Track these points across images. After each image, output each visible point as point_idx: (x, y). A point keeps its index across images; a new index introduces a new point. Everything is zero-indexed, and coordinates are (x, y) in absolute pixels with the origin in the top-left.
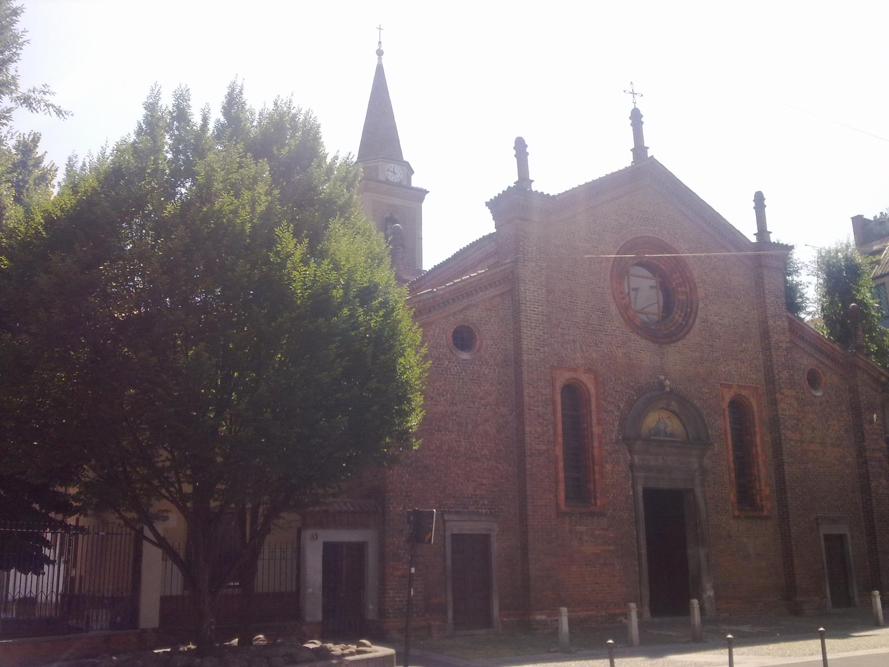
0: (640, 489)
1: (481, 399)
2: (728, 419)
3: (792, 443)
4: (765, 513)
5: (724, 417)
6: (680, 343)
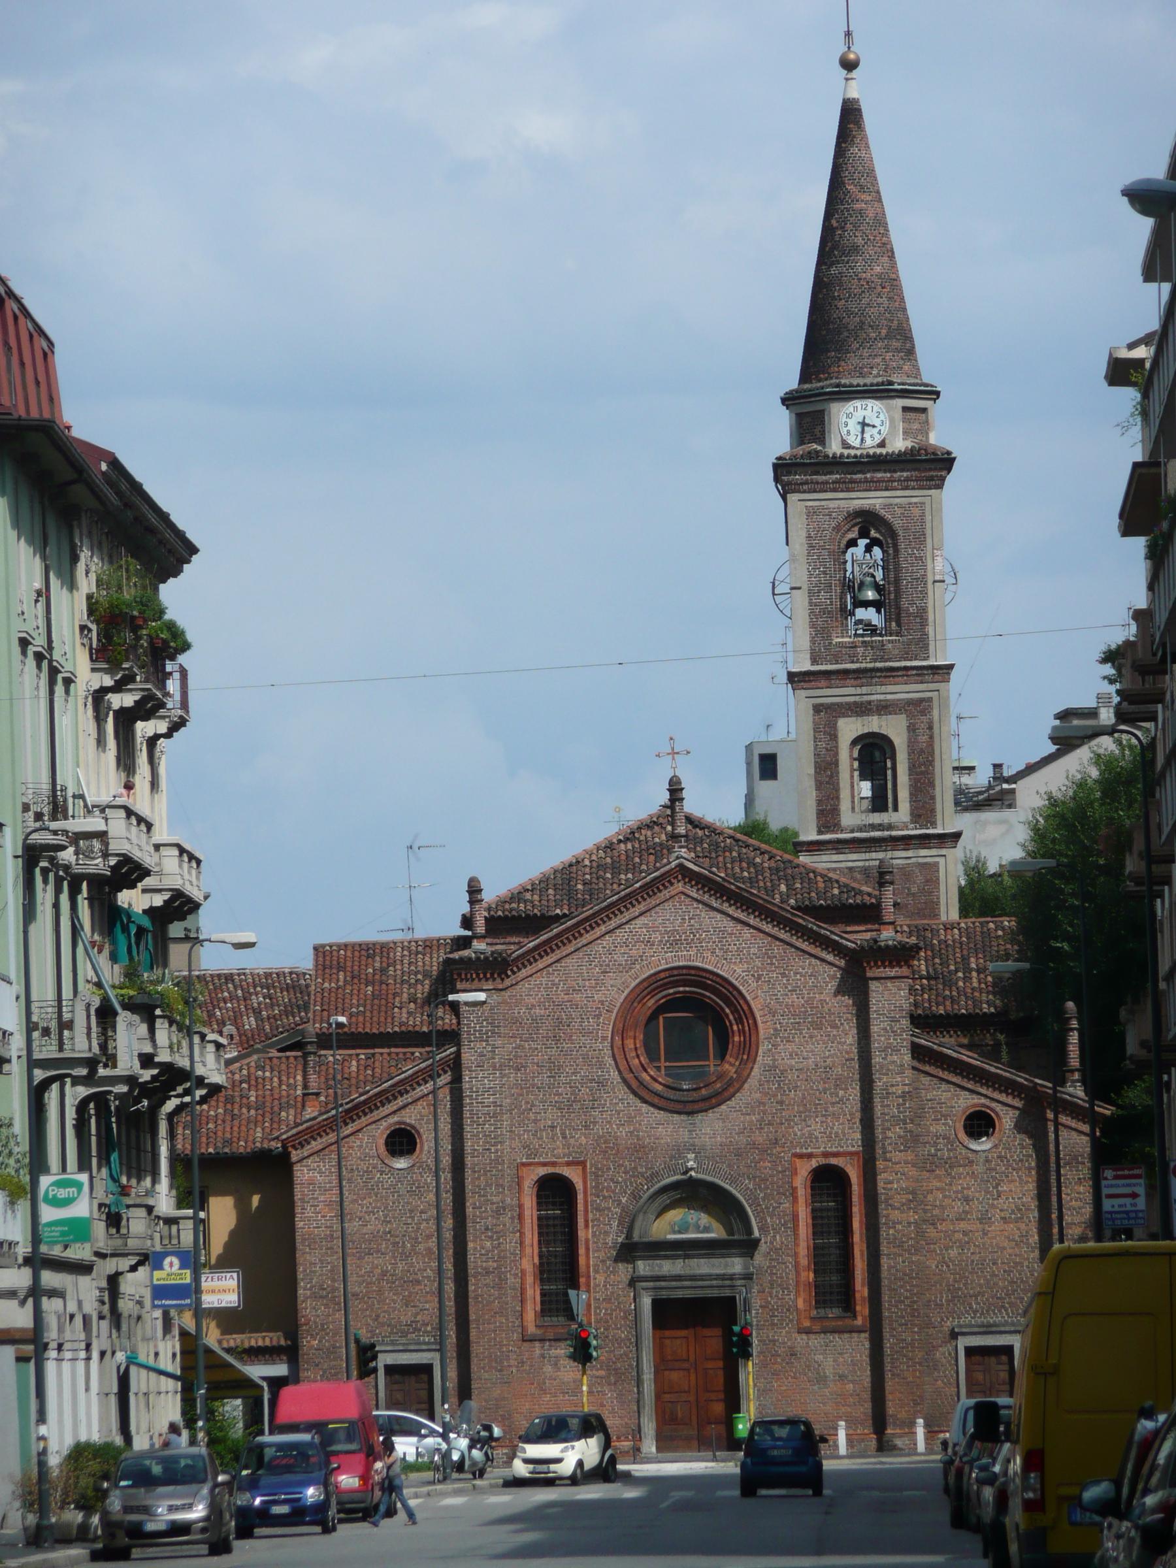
0: (647, 1302)
2: (801, 1200)
4: (859, 1321)
6: (723, 1107)
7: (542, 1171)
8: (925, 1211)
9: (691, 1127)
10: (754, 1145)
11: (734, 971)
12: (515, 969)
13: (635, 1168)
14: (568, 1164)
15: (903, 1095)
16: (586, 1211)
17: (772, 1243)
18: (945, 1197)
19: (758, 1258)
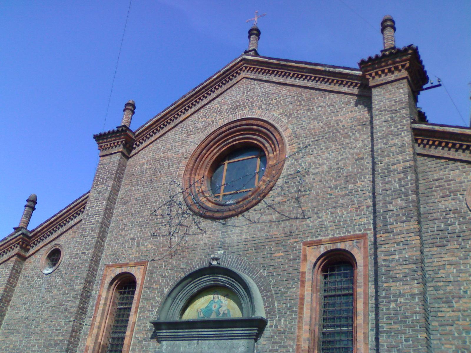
1: (48, 303)
3: (402, 300)
5: (303, 282)
7: (119, 271)
8: (437, 288)
9: (224, 229)
10: (271, 238)
11: (271, 116)
12: (138, 143)
13: (179, 264)
14: (136, 265)
15: (405, 171)
16: (139, 300)
17: (276, 327)
18: (460, 271)
19: (262, 341)
